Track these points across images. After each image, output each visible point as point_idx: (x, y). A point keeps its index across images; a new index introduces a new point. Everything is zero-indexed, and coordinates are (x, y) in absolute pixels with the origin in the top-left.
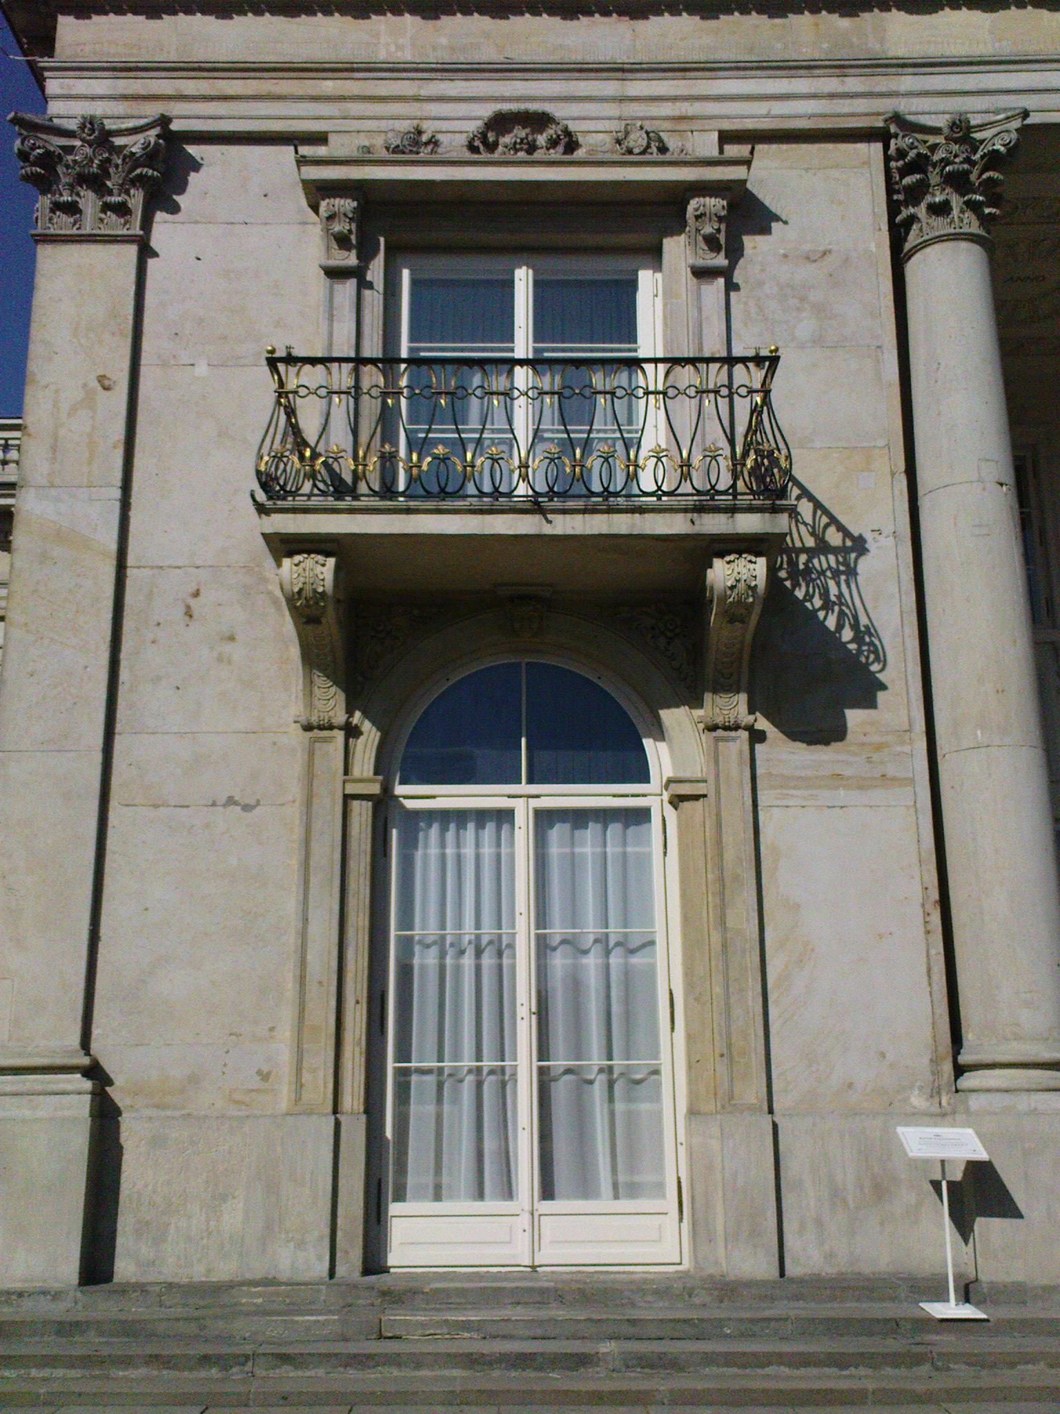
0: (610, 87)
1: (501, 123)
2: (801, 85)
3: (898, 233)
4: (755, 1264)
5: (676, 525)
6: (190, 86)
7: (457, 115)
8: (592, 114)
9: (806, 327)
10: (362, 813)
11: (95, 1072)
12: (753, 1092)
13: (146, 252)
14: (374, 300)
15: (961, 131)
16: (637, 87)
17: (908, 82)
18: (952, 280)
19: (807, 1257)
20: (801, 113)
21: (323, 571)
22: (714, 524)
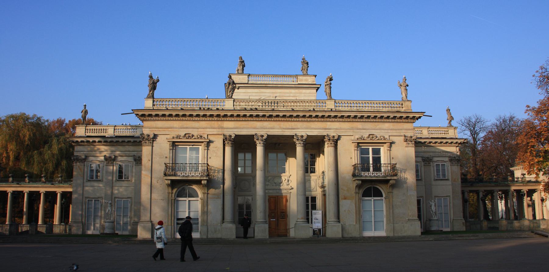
0: (197, 130)
1: (186, 134)
2: (215, 130)
3: (224, 145)
4: (205, 237)
5: (199, 178)
6: (156, 130)
7: (182, 134)
8: (195, 133)
9: (215, 155)
10: (173, 201)
11: (151, 222)
12: (205, 224)
13: (152, 146)
14: (174, 151)
15: (230, 136)
16: (200, 130)
17: (225, 130)
18: (228, 150)
19: (209, 236)
20: (215, 133)
21: (169, 182)
22: (202, 178)
